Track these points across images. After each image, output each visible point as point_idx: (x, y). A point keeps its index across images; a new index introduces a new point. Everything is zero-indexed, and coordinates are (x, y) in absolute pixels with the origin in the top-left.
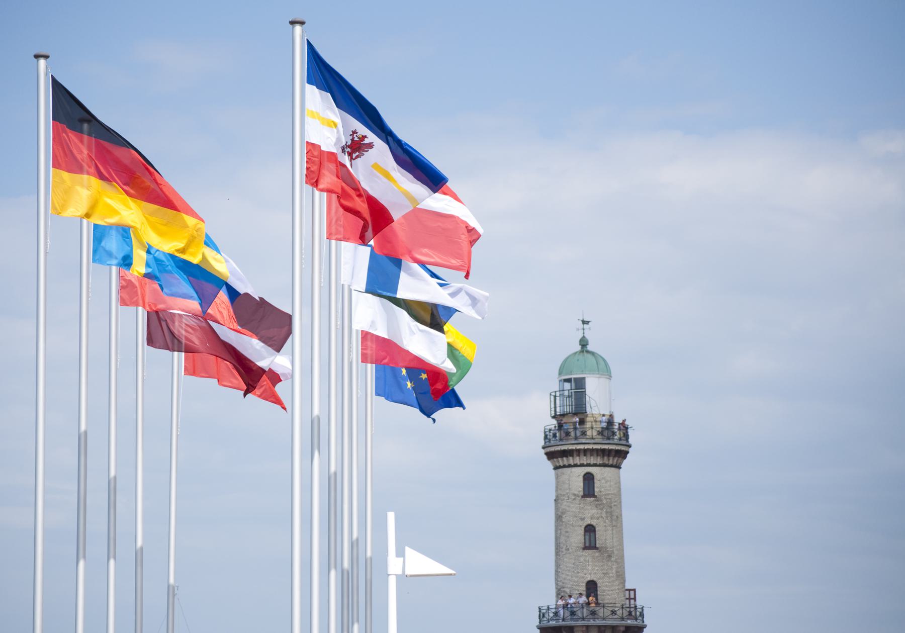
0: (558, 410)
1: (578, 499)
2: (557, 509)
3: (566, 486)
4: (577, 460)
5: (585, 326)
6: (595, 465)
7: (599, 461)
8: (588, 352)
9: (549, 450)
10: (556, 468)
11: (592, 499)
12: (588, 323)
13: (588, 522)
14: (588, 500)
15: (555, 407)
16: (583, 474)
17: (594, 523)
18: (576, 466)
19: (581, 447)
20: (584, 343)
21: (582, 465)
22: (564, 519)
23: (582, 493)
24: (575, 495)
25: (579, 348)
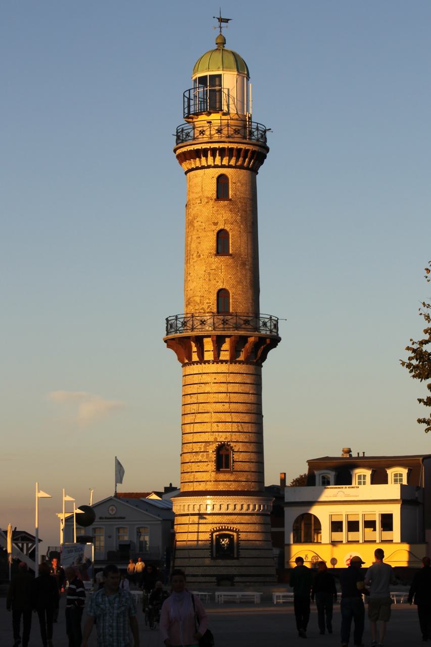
0: (192, 109)
1: (211, 203)
2: (188, 214)
3: (198, 189)
5: (223, 24)
9: (179, 151)
11: (226, 202)
12: (227, 21)
13: (221, 227)
14: (222, 203)
15: (189, 106)
16: (217, 176)
17: (227, 228)
18: (209, 167)
22: (196, 224)
23: (215, 196)
24: (208, 198)
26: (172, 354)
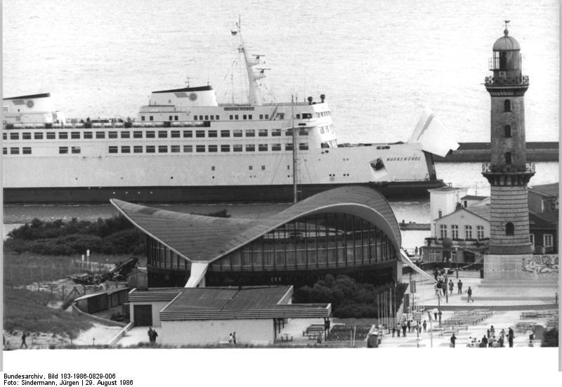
4: (502, 94)
6: (511, 96)
7: (512, 94)
8: (508, 37)
10: (492, 96)
19: (504, 88)
20: (506, 32)
21: (504, 96)
25: (503, 35)
26: (485, 180)
